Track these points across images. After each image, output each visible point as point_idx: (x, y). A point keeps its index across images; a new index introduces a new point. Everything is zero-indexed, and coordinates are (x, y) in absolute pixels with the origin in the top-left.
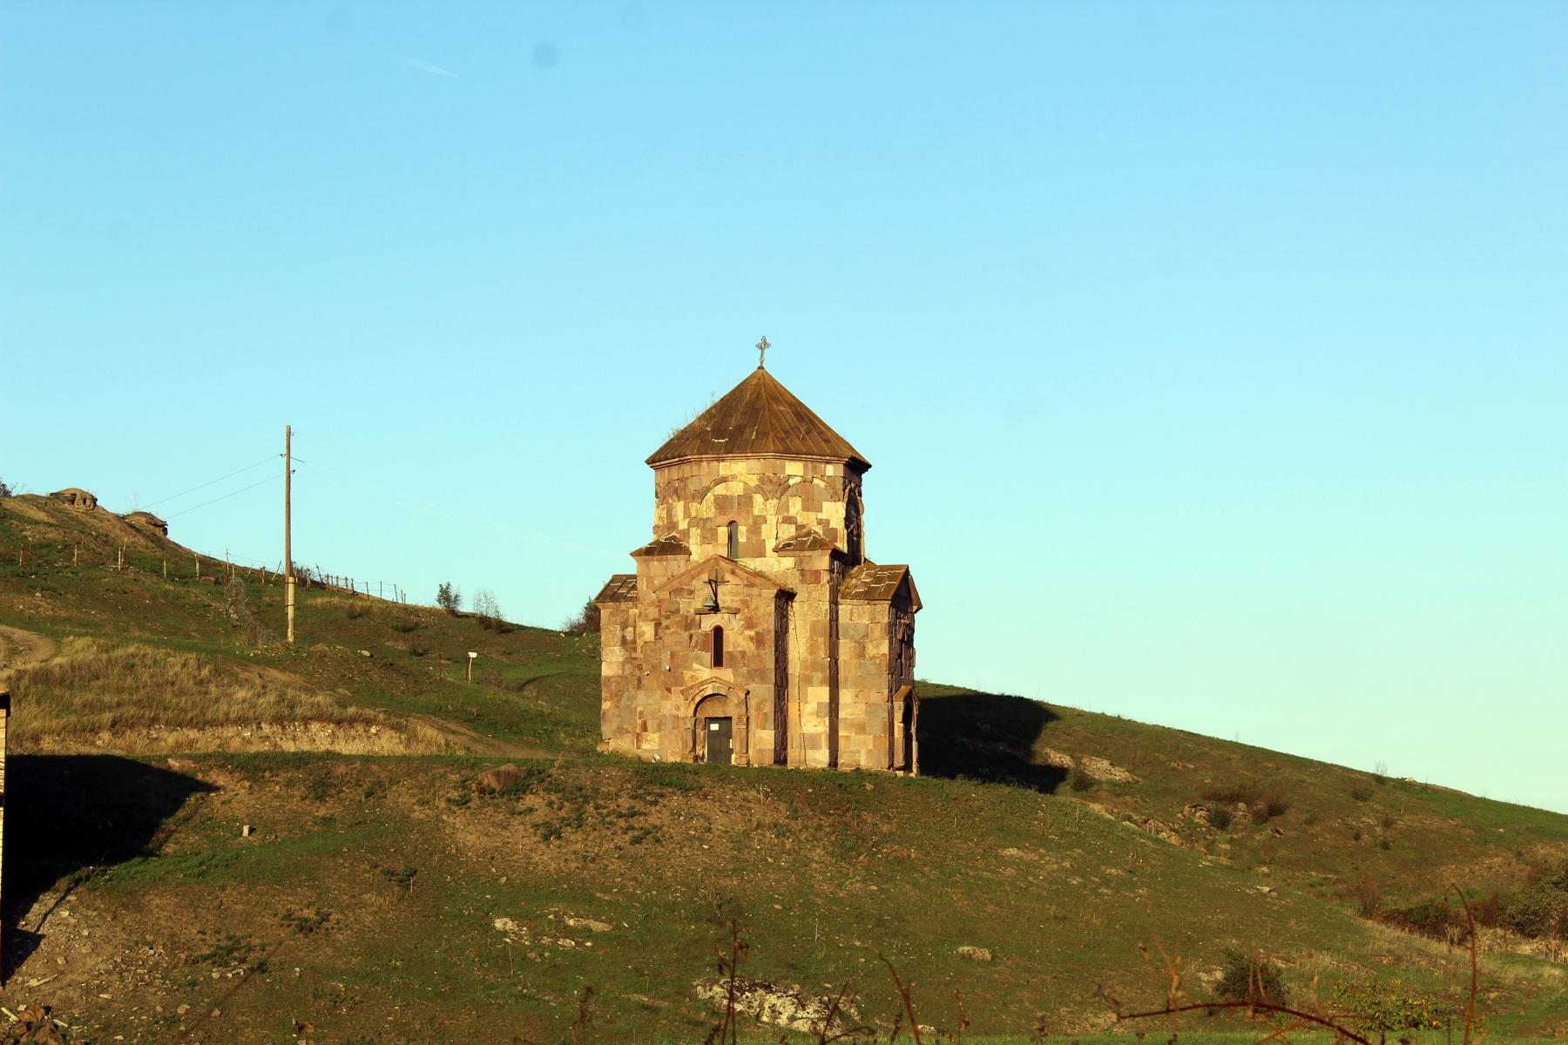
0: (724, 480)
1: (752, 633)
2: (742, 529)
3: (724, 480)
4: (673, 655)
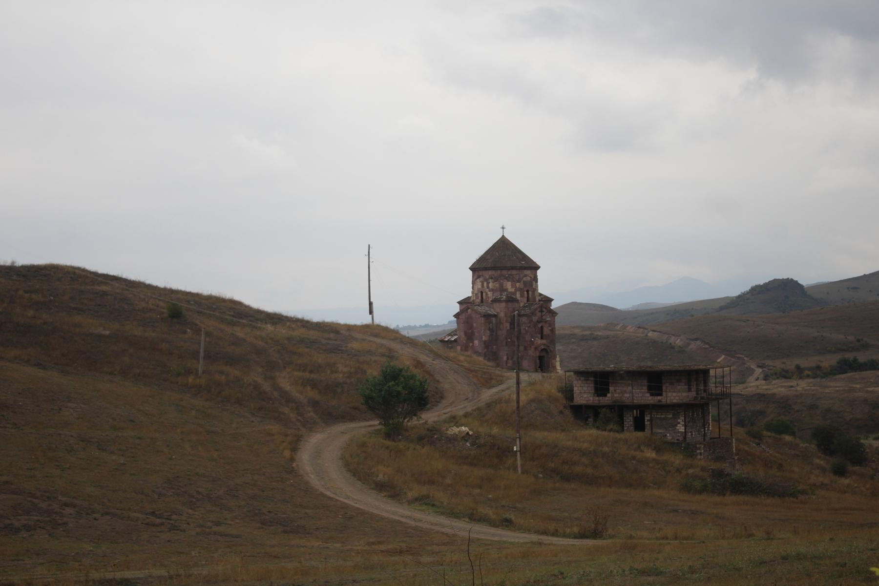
0: (526, 276)
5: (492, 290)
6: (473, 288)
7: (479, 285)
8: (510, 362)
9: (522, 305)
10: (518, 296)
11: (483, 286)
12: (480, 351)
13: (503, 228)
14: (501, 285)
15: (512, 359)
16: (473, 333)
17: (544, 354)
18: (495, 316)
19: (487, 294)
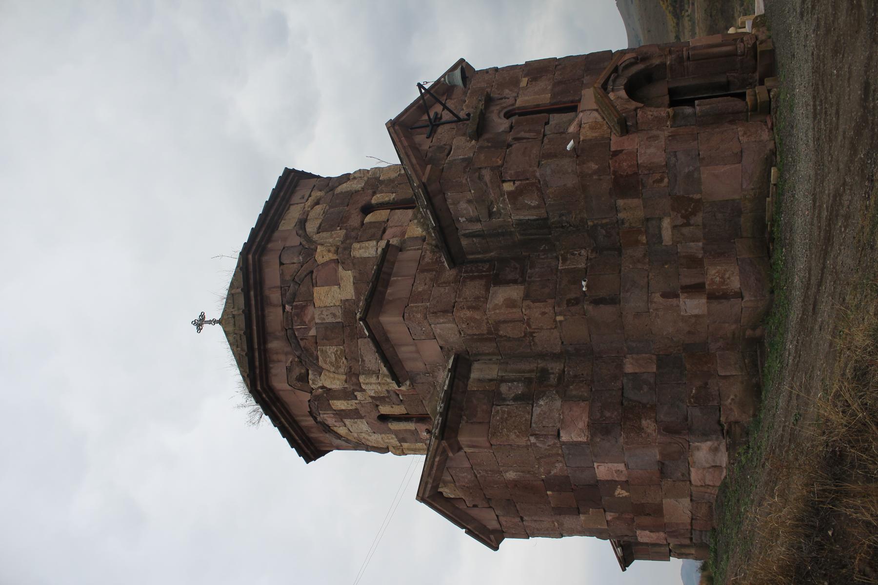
0: (302, 223)
1: (524, 82)
3: (302, 223)
5: (352, 375)
6: (383, 450)
7: (361, 428)
8: (713, 273)
9: (416, 231)
10: (368, 250)
11: (355, 414)
12: (655, 454)
13: (200, 323)
14: (330, 332)
15: (694, 262)
16: (561, 484)
18: (461, 365)
19: (378, 400)
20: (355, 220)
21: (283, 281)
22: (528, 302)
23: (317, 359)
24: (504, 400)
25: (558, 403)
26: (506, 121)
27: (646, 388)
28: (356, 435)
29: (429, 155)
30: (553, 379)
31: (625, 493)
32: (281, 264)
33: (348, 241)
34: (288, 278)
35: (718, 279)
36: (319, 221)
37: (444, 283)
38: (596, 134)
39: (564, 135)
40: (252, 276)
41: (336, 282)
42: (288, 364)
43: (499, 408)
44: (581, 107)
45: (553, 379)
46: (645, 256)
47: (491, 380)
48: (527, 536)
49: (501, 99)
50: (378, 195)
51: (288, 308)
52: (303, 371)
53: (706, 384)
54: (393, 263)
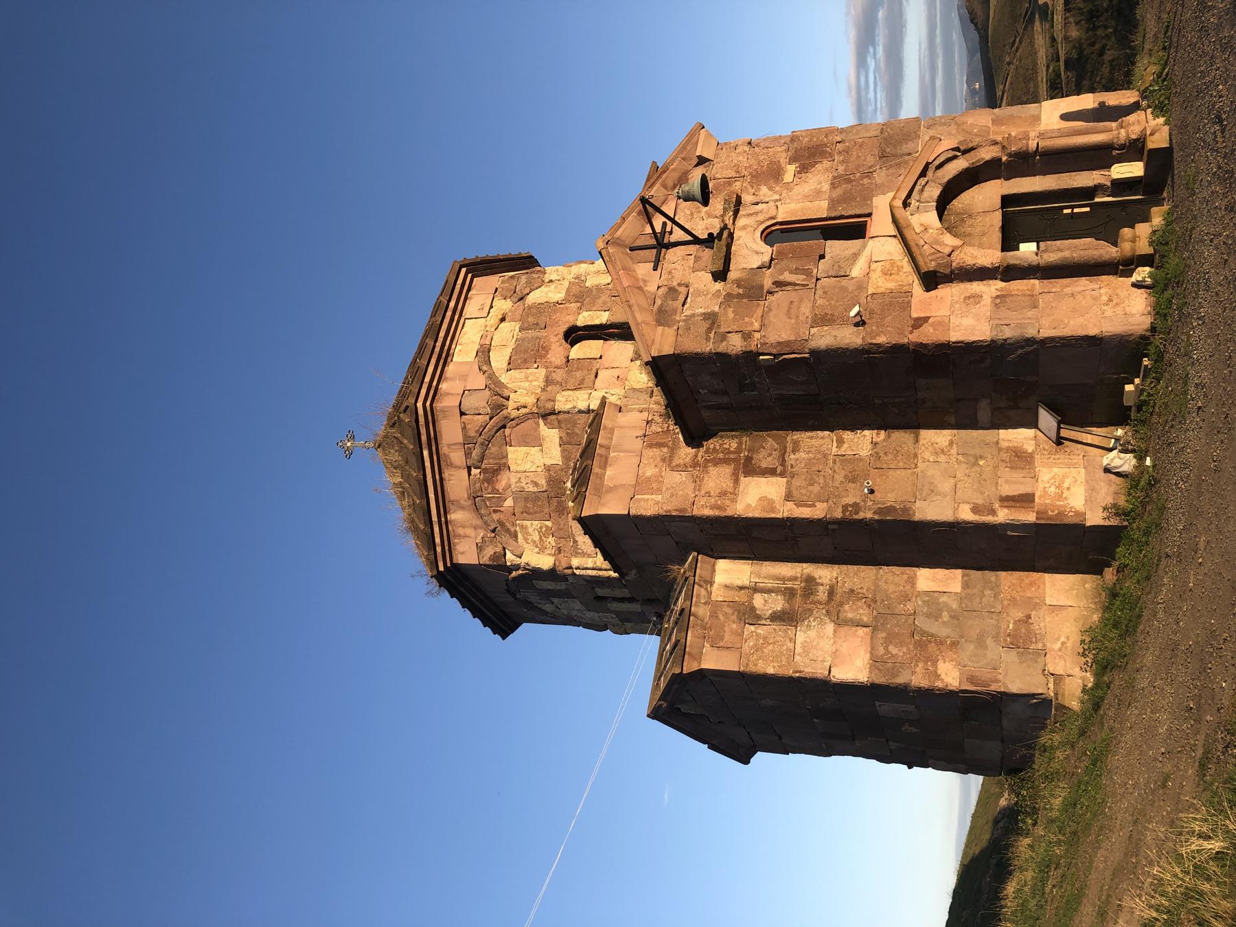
0: (484, 353)
1: (791, 169)
2: (585, 318)
3: (484, 353)
4: (822, 320)
6: (600, 628)
14: (531, 504)
17: (985, 198)
20: (557, 351)
21: (465, 436)
22: (790, 505)
23: (516, 536)
24: (759, 617)
25: (830, 627)
26: (766, 251)
27: (945, 616)
28: (565, 612)
29: (659, 302)
30: (822, 594)
31: (914, 730)
32: (462, 414)
33: (549, 388)
34: (472, 433)
35: (1053, 489)
36: (507, 352)
37: (679, 465)
38: (891, 285)
39: (844, 282)
40: (423, 431)
41: (537, 442)
42: (479, 540)
43: (752, 628)
44: (873, 229)
45: (822, 594)
46: (951, 443)
47: (741, 588)
48: (786, 752)
49: (757, 204)
50: (586, 314)
51: (474, 471)
52: (499, 549)
53: (1029, 617)
54: (612, 431)
